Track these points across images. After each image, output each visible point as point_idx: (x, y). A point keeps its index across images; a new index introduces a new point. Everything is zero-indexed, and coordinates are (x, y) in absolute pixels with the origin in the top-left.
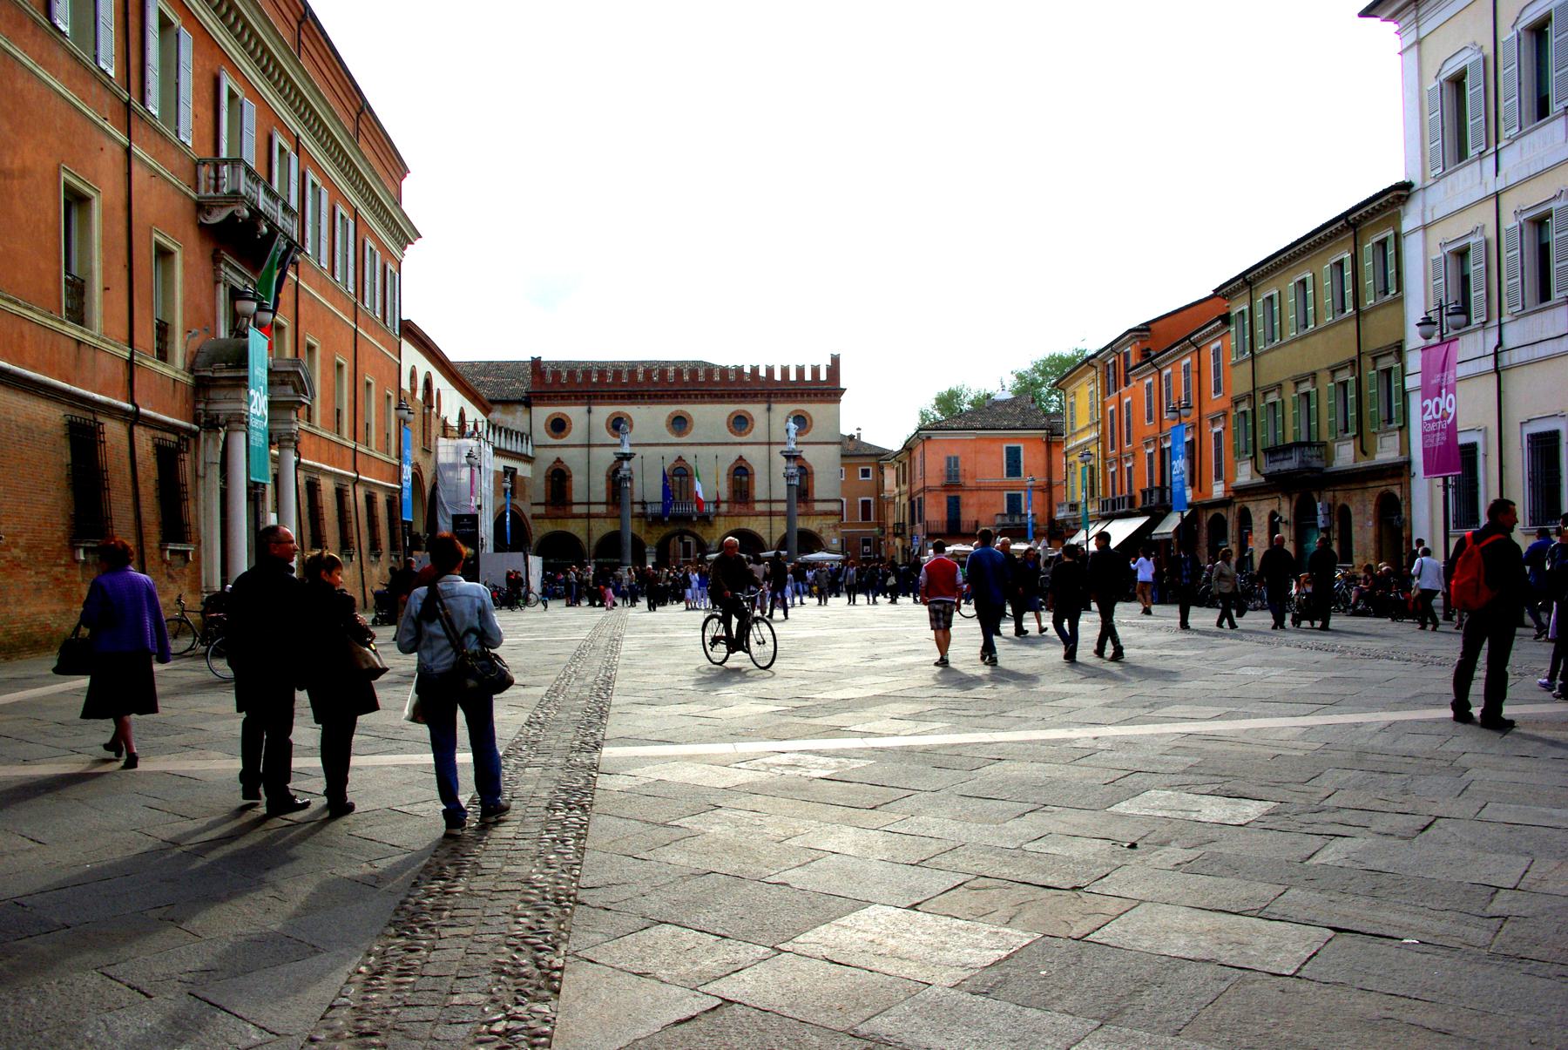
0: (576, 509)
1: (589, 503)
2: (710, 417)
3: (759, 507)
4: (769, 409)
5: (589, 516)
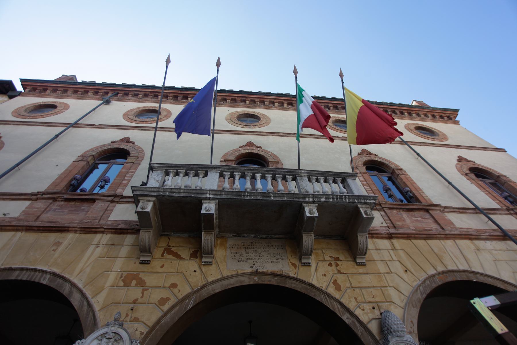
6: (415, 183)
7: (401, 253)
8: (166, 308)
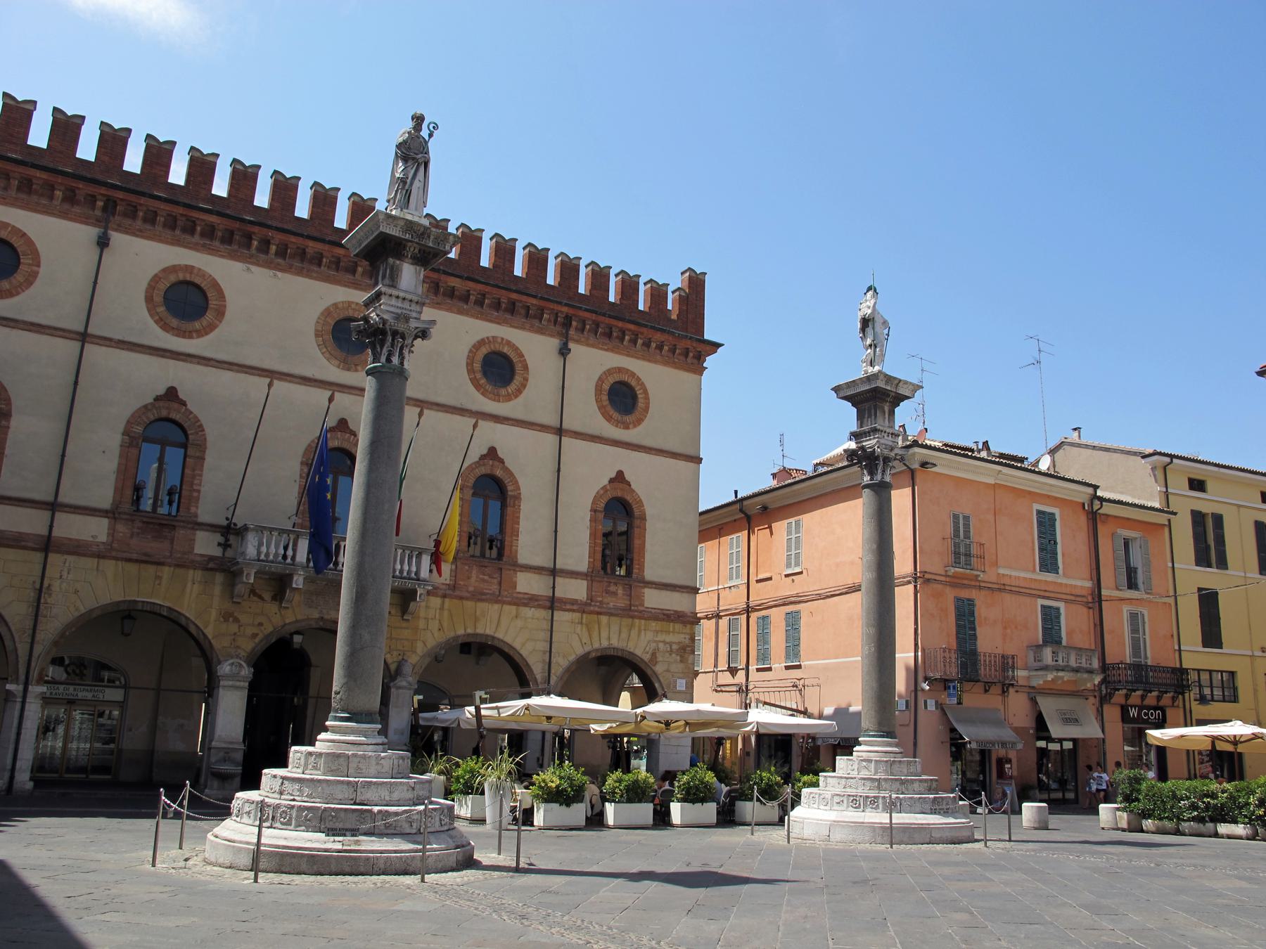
1: (53, 506)
3: (527, 584)
4: (564, 352)
5: (47, 545)
6: (518, 523)
7: (446, 613)
8: (257, 640)
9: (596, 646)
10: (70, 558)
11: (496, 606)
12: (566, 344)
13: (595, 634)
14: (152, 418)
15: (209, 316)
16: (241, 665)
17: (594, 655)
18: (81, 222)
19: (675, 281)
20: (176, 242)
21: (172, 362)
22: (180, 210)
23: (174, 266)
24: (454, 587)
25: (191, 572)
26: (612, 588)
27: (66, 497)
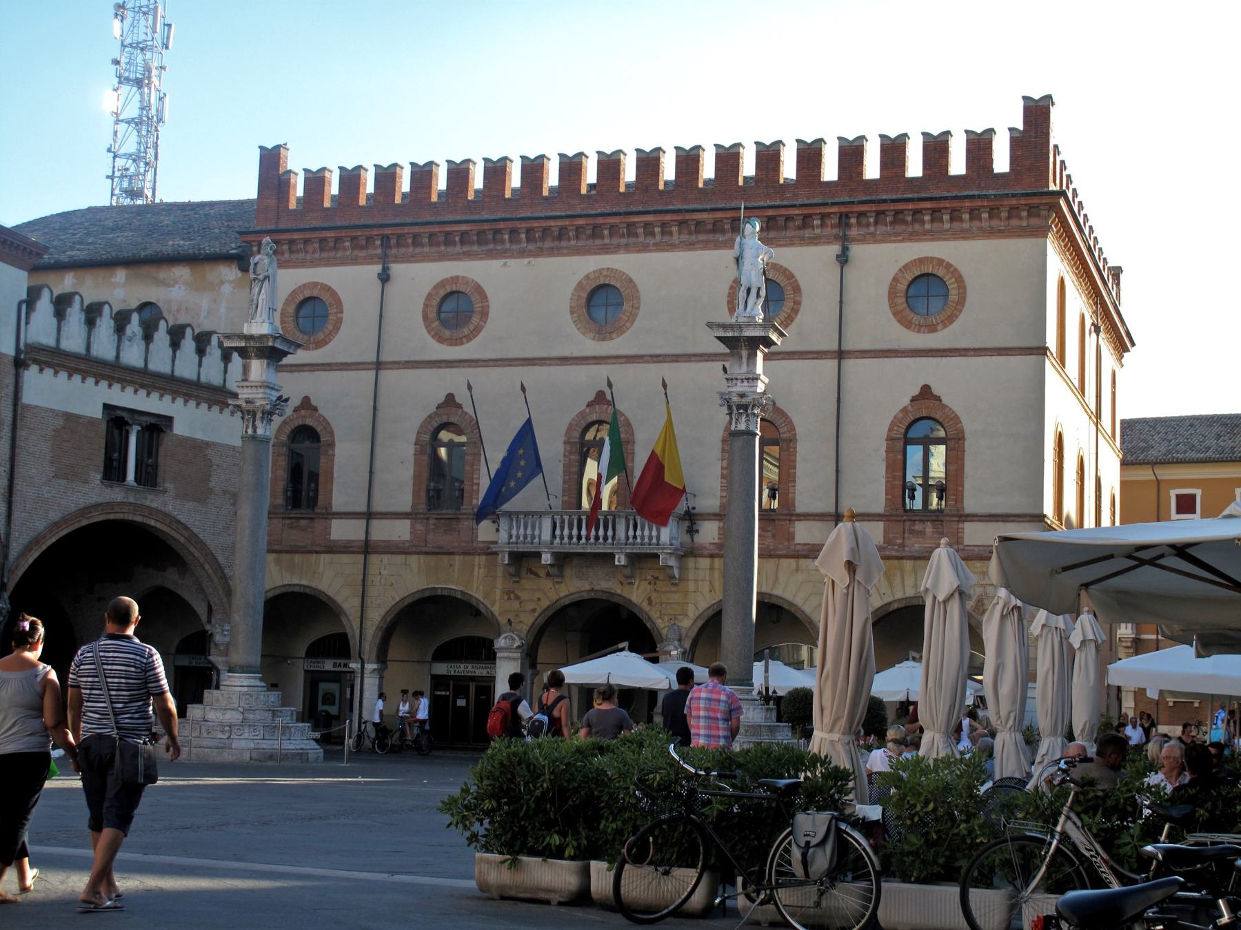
0: (341, 531)
1: (369, 515)
2: (678, 283)
4: (843, 259)
5: (367, 548)
6: (795, 468)
8: (537, 614)
9: (899, 595)
10: (386, 557)
11: (772, 560)
12: (845, 250)
13: (898, 581)
14: (436, 425)
15: (476, 319)
16: (514, 639)
17: (896, 606)
18: (369, 264)
19: (1006, 119)
20: (441, 257)
21: (447, 370)
22: (436, 229)
23: (443, 281)
24: (720, 546)
25: (477, 558)
26: (918, 527)
27: (378, 507)
